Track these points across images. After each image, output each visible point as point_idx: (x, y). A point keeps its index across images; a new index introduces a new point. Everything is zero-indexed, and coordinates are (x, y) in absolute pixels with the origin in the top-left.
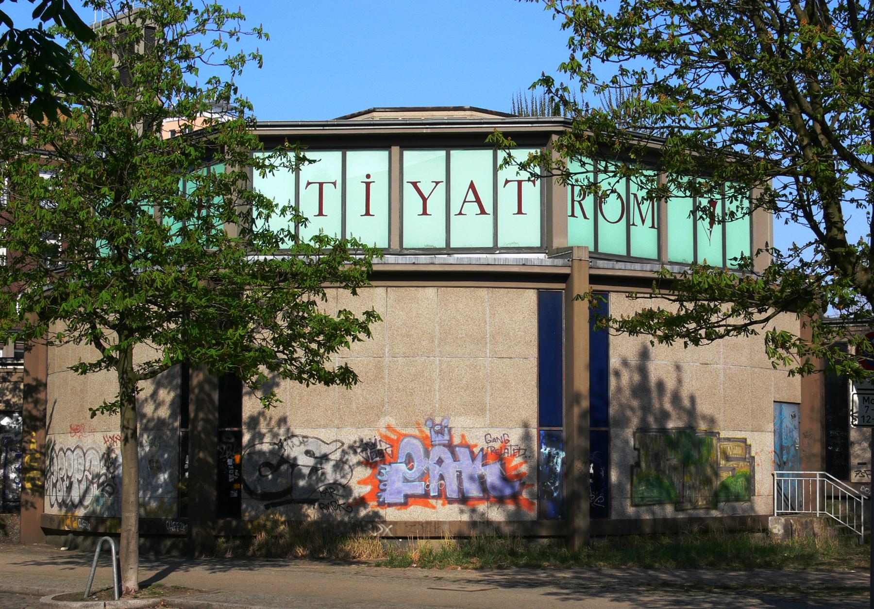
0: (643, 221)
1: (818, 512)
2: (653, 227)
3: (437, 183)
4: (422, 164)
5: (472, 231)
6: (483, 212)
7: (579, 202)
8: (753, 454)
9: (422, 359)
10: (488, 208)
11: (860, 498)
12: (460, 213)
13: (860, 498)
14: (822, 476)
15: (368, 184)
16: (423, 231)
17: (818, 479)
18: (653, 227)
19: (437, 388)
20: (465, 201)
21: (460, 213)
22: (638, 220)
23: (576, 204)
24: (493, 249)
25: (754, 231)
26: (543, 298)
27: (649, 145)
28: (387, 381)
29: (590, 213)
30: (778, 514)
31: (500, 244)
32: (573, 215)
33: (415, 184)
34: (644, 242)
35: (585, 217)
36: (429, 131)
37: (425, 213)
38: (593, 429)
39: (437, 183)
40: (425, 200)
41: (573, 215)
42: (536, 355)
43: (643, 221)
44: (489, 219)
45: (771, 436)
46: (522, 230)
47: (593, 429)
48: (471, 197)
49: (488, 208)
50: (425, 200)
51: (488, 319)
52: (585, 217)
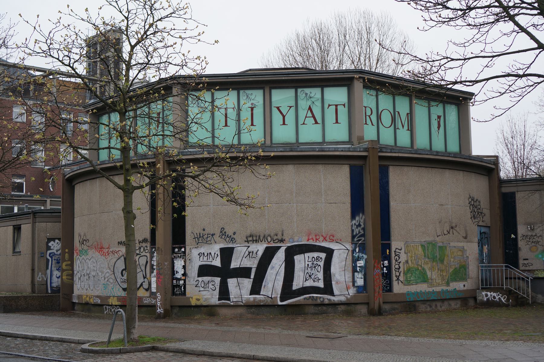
0: (403, 127)
1: (505, 287)
2: (408, 130)
3: (291, 107)
4: (282, 97)
5: (310, 134)
6: (316, 122)
7: (369, 116)
8: (468, 255)
9: (287, 205)
10: (319, 120)
11: (528, 278)
12: (304, 124)
13: (528, 278)
14: (506, 266)
15: (252, 109)
16: (283, 134)
17: (504, 268)
18: (408, 130)
19: (295, 220)
20: (306, 117)
21: (304, 124)
22: (400, 126)
23: (368, 117)
24: (324, 142)
25: (461, 132)
26: (352, 168)
27: (404, 84)
28: (267, 217)
29: (375, 122)
30: (482, 288)
31: (327, 140)
32: (366, 124)
33: (278, 108)
34: (404, 139)
35: (373, 125)
36: (286, 78)
37: (284, 124)
38: (389, 242)
39: (291, 107)
40: (284, 117)
41: (366, 124)
42: (350, 201)
43: (403, 127)
44: (319, 126)
45: (477, 245)
46: (337, 133)
47: (389, 242)
48: (310, 114)
49: (319, 120)
50: (284, 117)
51: (322, 182)
52: (373, 125)
